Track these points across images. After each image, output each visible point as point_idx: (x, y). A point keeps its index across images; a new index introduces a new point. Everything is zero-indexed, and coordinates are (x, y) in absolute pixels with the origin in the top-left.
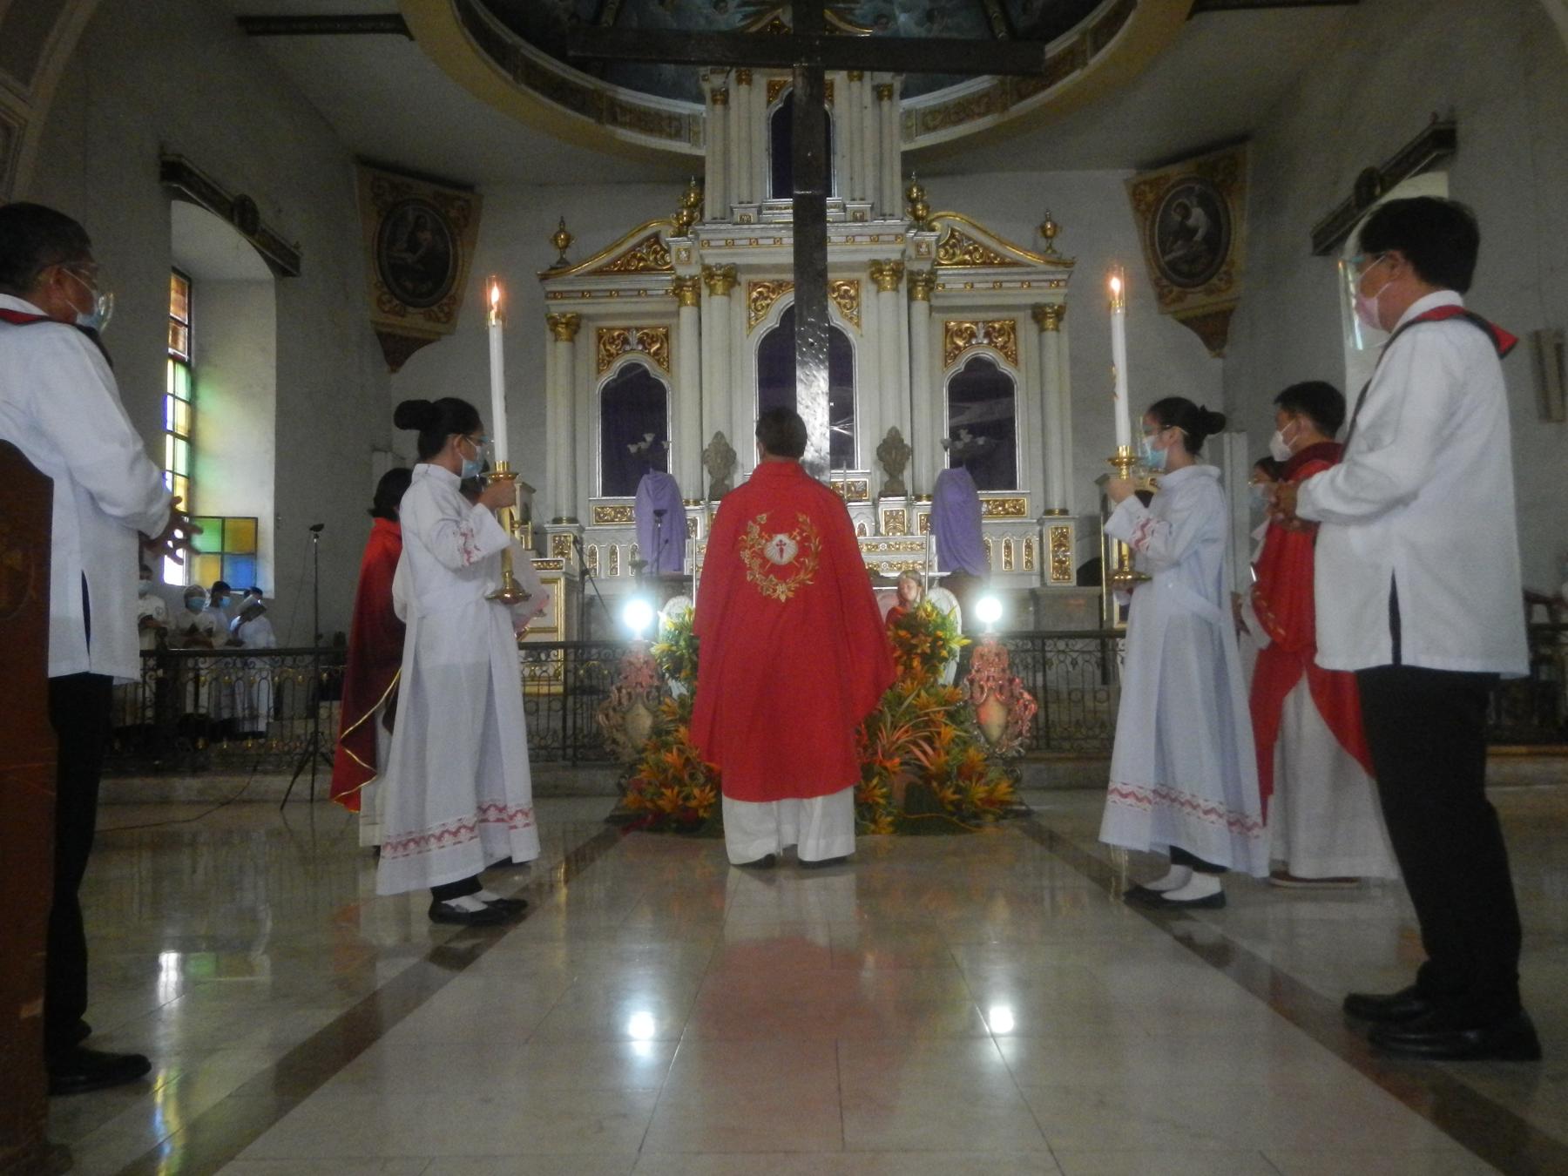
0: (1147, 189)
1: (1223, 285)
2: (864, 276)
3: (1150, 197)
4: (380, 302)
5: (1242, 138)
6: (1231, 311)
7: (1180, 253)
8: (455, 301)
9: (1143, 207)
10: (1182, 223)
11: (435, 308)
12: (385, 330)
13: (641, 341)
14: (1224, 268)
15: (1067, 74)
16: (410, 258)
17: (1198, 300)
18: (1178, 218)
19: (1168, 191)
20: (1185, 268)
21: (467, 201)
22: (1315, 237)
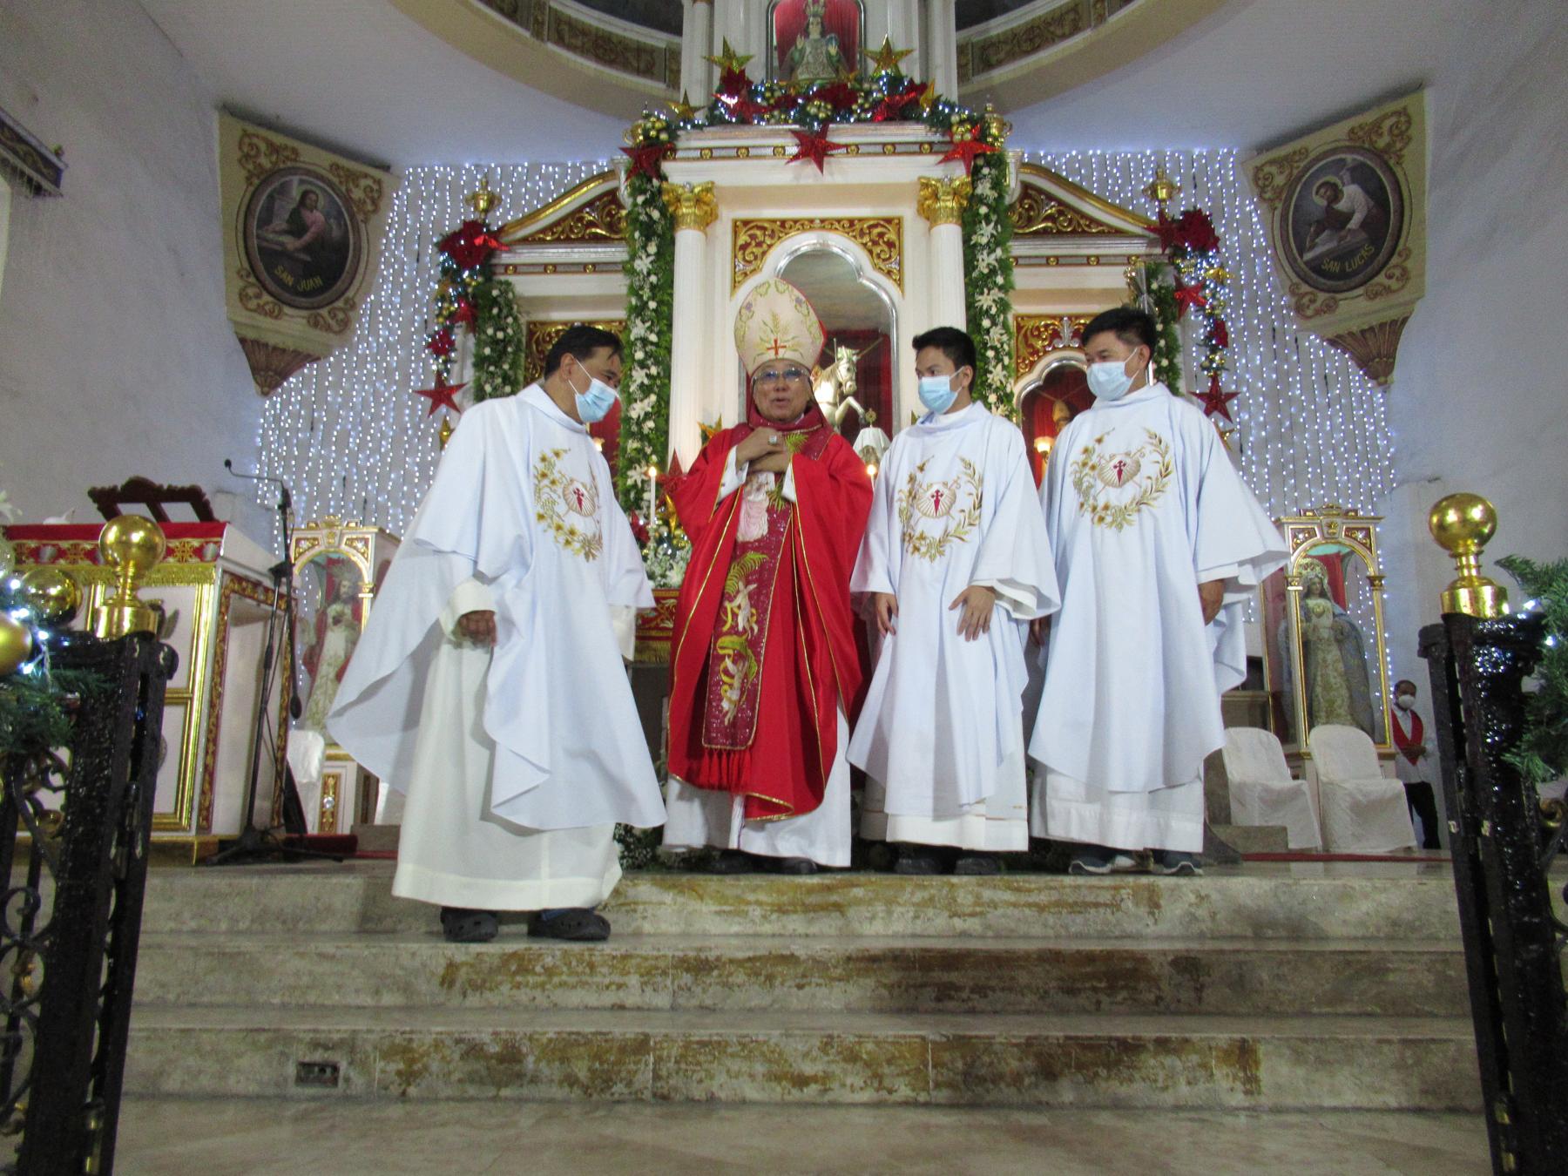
0: (1274, 169)
1: (1394, 284)
2: (907, 212)
3: (1280, 180)
4: (243, 297)
5: (1415, 87)
6: (1405, 320)
8: (352, 305)
9: (1267, 196)
10: (1329, 208)
11: (324, 312)
12: (251, 335)
14: (1395, 260)
16: (291, 243)
17: (1356, 309)
18: (1323, 203)
19: (1307, 169)
20: (1335, 267)
21: (379, 182)
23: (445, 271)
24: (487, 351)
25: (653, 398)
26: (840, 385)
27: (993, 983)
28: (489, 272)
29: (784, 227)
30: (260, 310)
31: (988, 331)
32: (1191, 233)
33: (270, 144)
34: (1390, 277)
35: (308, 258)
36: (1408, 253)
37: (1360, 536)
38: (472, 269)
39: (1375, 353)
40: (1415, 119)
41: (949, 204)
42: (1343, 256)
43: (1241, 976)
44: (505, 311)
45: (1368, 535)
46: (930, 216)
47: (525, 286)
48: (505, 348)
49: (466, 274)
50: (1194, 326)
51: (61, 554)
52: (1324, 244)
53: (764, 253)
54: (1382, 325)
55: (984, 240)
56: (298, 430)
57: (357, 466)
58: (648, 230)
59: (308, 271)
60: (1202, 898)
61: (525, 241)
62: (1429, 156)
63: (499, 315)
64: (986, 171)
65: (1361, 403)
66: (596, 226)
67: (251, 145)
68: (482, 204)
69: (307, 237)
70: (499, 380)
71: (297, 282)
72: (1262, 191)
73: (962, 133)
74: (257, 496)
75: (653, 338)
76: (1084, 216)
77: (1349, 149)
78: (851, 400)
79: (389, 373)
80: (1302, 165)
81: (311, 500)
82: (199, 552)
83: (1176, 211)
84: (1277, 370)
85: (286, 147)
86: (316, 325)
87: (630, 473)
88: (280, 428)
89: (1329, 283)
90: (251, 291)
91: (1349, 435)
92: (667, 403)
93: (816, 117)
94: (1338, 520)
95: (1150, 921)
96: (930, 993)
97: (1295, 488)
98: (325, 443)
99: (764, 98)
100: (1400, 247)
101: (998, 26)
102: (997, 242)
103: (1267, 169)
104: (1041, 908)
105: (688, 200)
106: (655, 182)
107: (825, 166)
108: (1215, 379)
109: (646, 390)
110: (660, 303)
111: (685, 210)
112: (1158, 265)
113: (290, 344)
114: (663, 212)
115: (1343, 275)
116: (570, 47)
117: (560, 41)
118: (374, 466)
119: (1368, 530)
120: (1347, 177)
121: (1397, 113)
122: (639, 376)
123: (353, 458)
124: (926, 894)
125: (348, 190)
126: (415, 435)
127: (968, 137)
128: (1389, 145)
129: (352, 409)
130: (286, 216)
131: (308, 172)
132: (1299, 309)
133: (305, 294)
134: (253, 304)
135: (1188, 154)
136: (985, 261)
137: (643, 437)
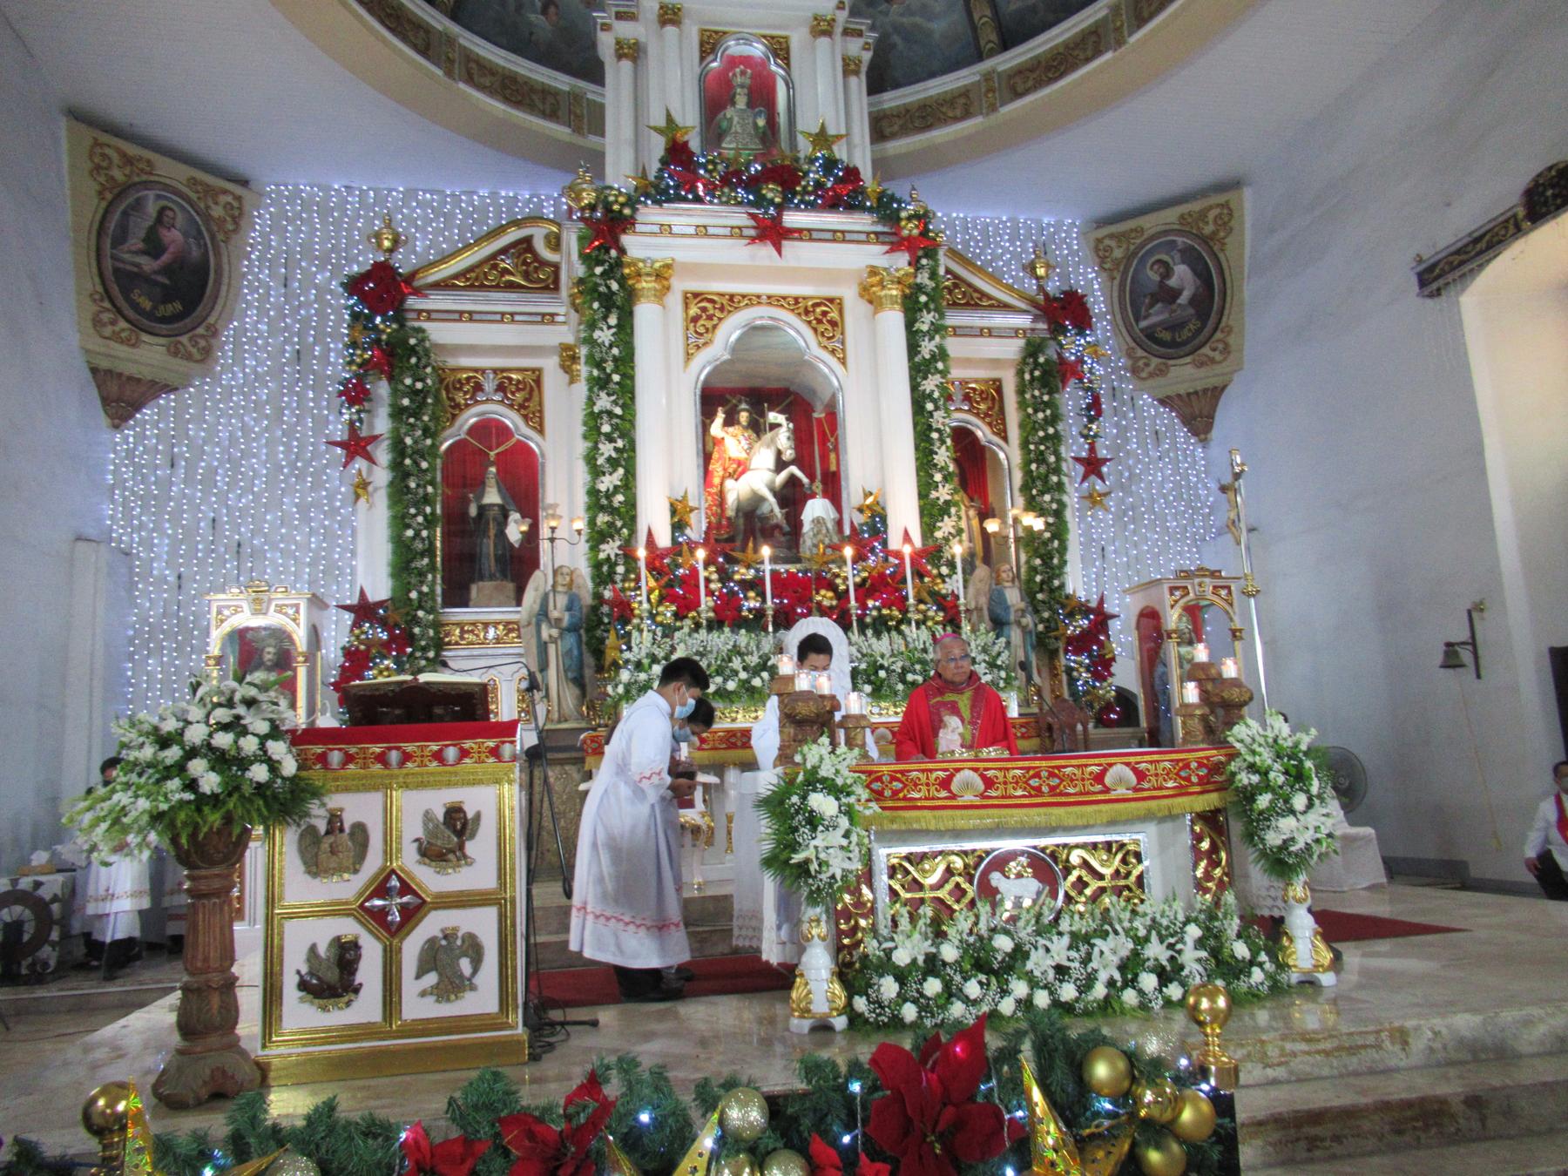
0: (1113, 243)
1: (1217, 356)
3: (1118, 253)
4: (97, 323)
7: (1161, 318)
10: (1162, 284)
11: (184, 339)
12: (104, 364)
13: (501, 388)
14: (1218, 335)
15: (1088, 60)
16: (148, 264)
17: (1184, 375)
18: (1156, 278)
20: (1166, 336)
21: (239, 198)
22: (1420, 275)
23: (355, 316)
24: (406, 402)
25: (621, 471)
26: (779, 453)
27: (1346, 1131)
28: (400, 319)
29: (732, 302)
30: (116, 337)
31: (931, 414)
32: (1065, 311)
33: (123, 155)
34: (1214, 350)
35: (167, 282)
36: (1229, 330)
37: (1223, 593)
38: (384, 314)
39: (1197, 414)
40: (1236, 215)
41: (894, 292)
42: (1174, 327)
43: (1509, 1106)
44: (424, 361)
45: (1230, 593)
46: (875, 303)
47: (438, 333)
48: (425, 398)
49: (378, 320)
50: (1071, 399)
51: (349, 759)
52: (1158, 315)
53: (715, 327)
54: (1205, 391)
55: (925, 328)
56: (156, 467)
57: (228, 507)
58: (608, 302)
59: (167, 296)
60: (1436, 1034)
61: (438, 286)
62: (1248, 246)
63: (417, 365)
64: (924, 261)
65: (1186, 456)
66: (512, 274)
67: (104, 155)
68: (387, 244)
69: (166, 258)
70: (419, 433)
71: (155, 308)
72: (1102, 261)
73: (910, 229)
74: (111, 540)
75: (618, 411)
76: (977, 290)
77: (1179, 232)
78: (794, 469)
79: (259, 406)
80: (1138, 241)
81: (175, 544)
82: (495, 752)
83: (1053, 287)
84: (1117, 425)
85: (140, 159)
86: (175, 354)
87: (602, 547)
88: (134, 463)
89: (1163, 350)
90: (106, 317)
91: (1177, 485)
92: (634, 476)
93: (771, 202)
94: (1207, 580)
95: (1403, 1056)
96: (1303, 1144)
97: (1134, 532)
98: (189, 480)
99: (706, 171)
100: (1223, 324)
101: (893, 99)
102: (937, 329)
103: (1107, 242)
104: (1327, 1053)
105: (648, 275)
106: (613, 253)
107: (784, 251)
108: (1092, 449)
109: (614, 463)
110: (623, 376)
111: (646, 284)
112: (1044, 339)
113: (146, 373)
114: (622, 281)
115: (1173, 344)
116: (481, 88)
117: (470, 80)
118: (247, 508)
119: (1229, 588)
120: (1177, 257)
121: (1222, 206)
122: (607, 449)
123: (223, 498)
124: (1244, 1051)
125: (208, 207)
126: (291, 474)
127: (915, 232)
128: (1215, 233)
129: (218, 444)
130: (142, 234)
131: (166, 187)
132: (1135, 371)
133: (164, 320)
134: (108, 331)
135: (1039, 222)
136: (927, 348)
137: (613, 511)
